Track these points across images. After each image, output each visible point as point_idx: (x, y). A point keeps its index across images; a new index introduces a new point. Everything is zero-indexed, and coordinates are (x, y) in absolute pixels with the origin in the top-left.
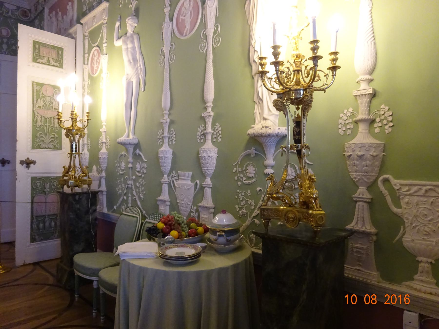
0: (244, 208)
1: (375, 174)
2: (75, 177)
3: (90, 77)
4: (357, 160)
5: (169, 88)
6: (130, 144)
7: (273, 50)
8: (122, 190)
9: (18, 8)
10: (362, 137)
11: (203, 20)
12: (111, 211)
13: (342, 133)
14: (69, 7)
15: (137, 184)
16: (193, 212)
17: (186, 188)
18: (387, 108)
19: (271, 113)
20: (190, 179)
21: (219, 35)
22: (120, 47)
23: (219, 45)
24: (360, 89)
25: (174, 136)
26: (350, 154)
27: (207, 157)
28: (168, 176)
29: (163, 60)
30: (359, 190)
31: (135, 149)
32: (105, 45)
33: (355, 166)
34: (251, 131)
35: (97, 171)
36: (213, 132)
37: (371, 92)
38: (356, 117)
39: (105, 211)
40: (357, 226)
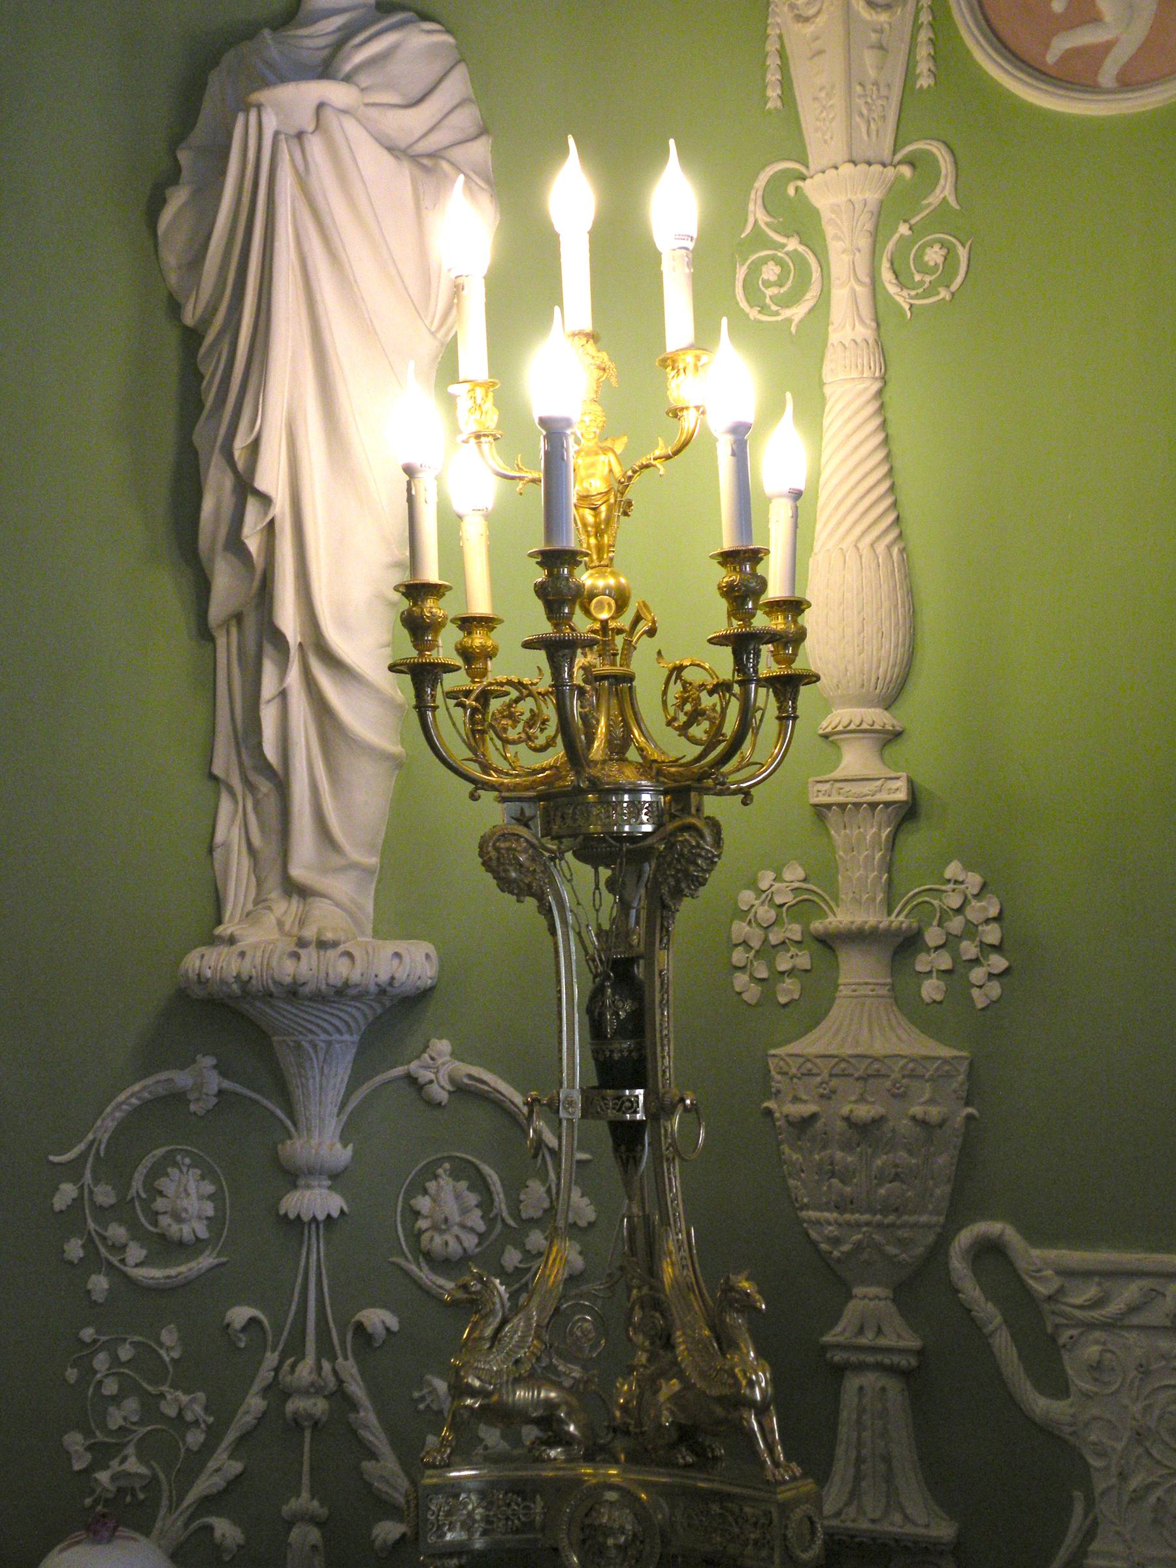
0: (130, 1450)
1: (934, 1219)
4: (847, 1147)
7: (541, 575)
10: (859, 1023)
13: (752, 993)
18: (974, 880)
19: (335, 860)
24: (837, 774)
26: (811, 1108)
30: (853, 1310)
33: (833, 1174)
34: (209, 963)
37: (902, 796)
38: (826, 916)
40: (861, 1510)
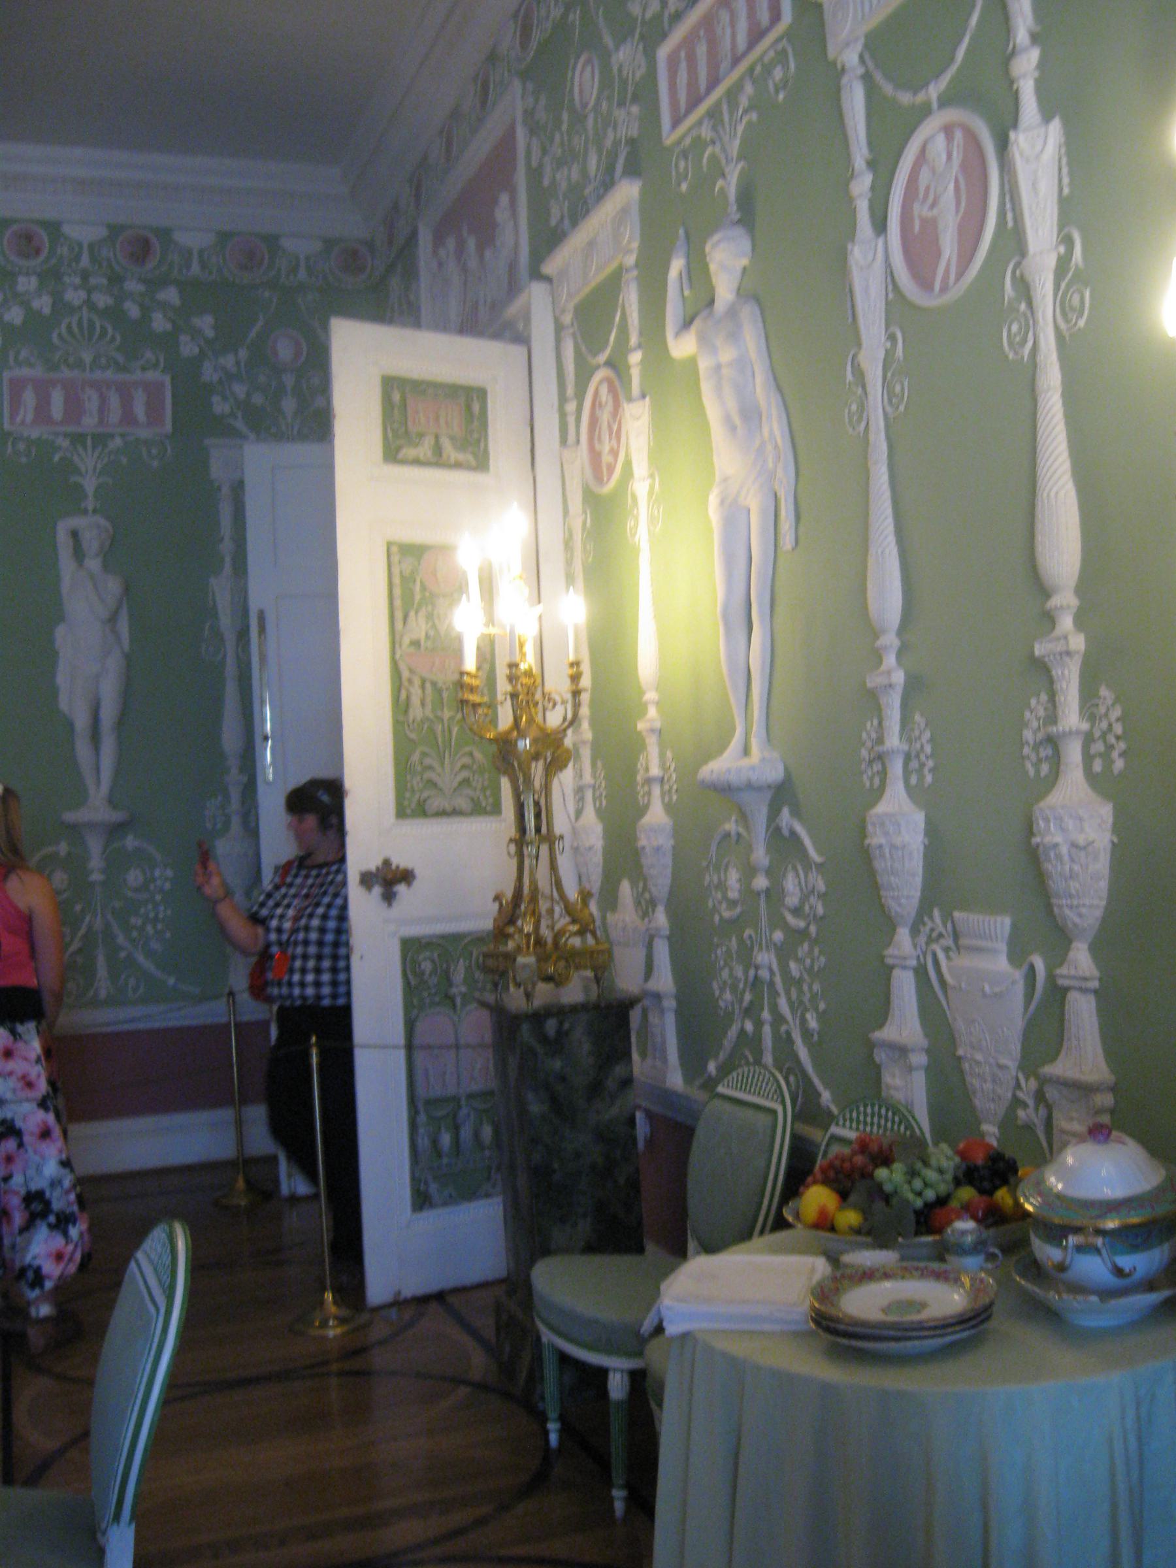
2: (539, 942)
3: (592, 500)
5: (891, 528)
6: (749, 786)
8: (734, 988)
9: (329, 243)
11: (1009, 216)
12: (697, 1083)
14: (501, 214)
15: (793, 965)
16: (1025, 1105)
17: (987, 988)
20: (1003, 947)
21: (1080, 279)
22: (692, 362)
23: (1082, 323)
25: (928, 749)
27: (1064, 850)
28: (915, 932)
29: (862, 407)
31: (774, 813)
32: (635, 358)
35: (638, 903)
36: (1085, 726)
39: (675, 1080)
